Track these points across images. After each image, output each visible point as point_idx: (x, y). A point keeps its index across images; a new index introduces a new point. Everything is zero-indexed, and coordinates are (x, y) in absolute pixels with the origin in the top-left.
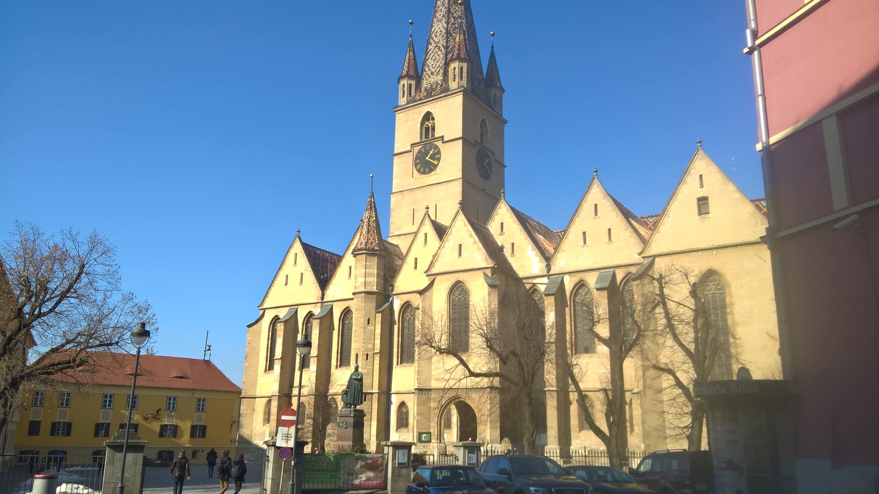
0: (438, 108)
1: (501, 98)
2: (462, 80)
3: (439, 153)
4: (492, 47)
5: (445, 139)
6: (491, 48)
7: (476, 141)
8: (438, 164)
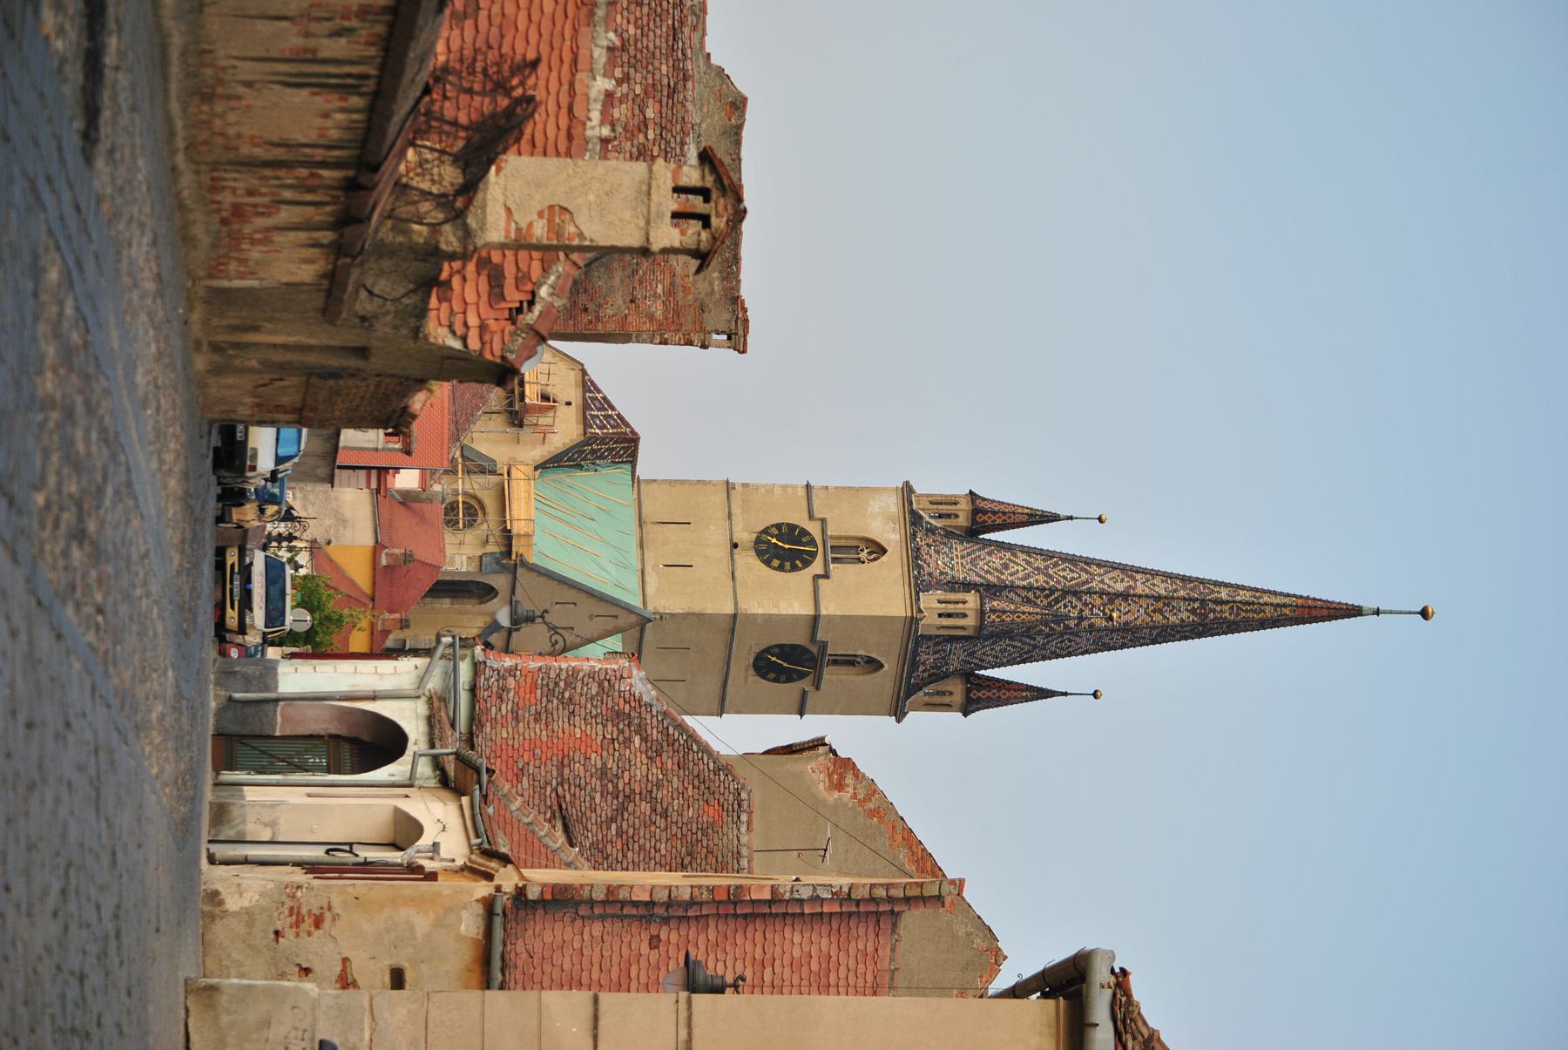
0: (892, 569)
2: (940, 615)
3: (794, 568)
4: (1066, 694)
5: (822, 582)
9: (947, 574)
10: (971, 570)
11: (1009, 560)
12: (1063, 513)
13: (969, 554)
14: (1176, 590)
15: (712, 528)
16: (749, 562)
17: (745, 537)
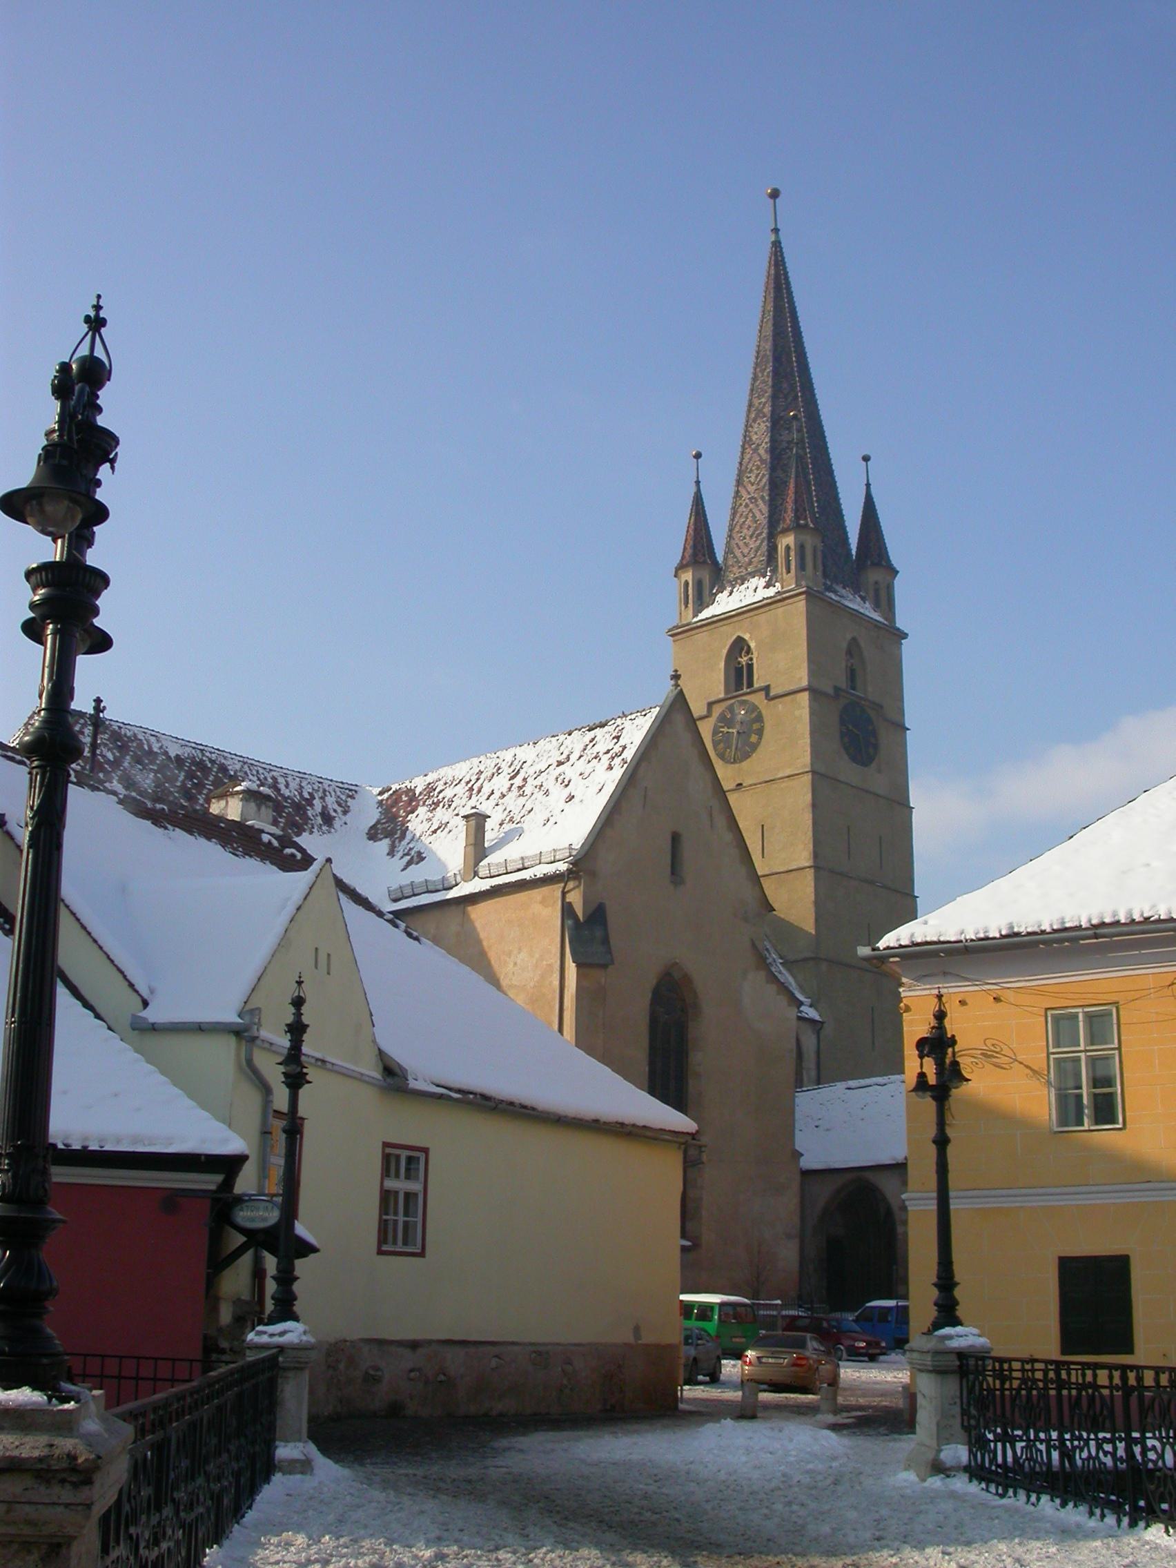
1: (890, 589)
3: (759, 719)
4: (868, 485)
5: (772, 694)
6: (865, 487)
7: (837, 689)
8: (759, 743)
12: (693, 489)
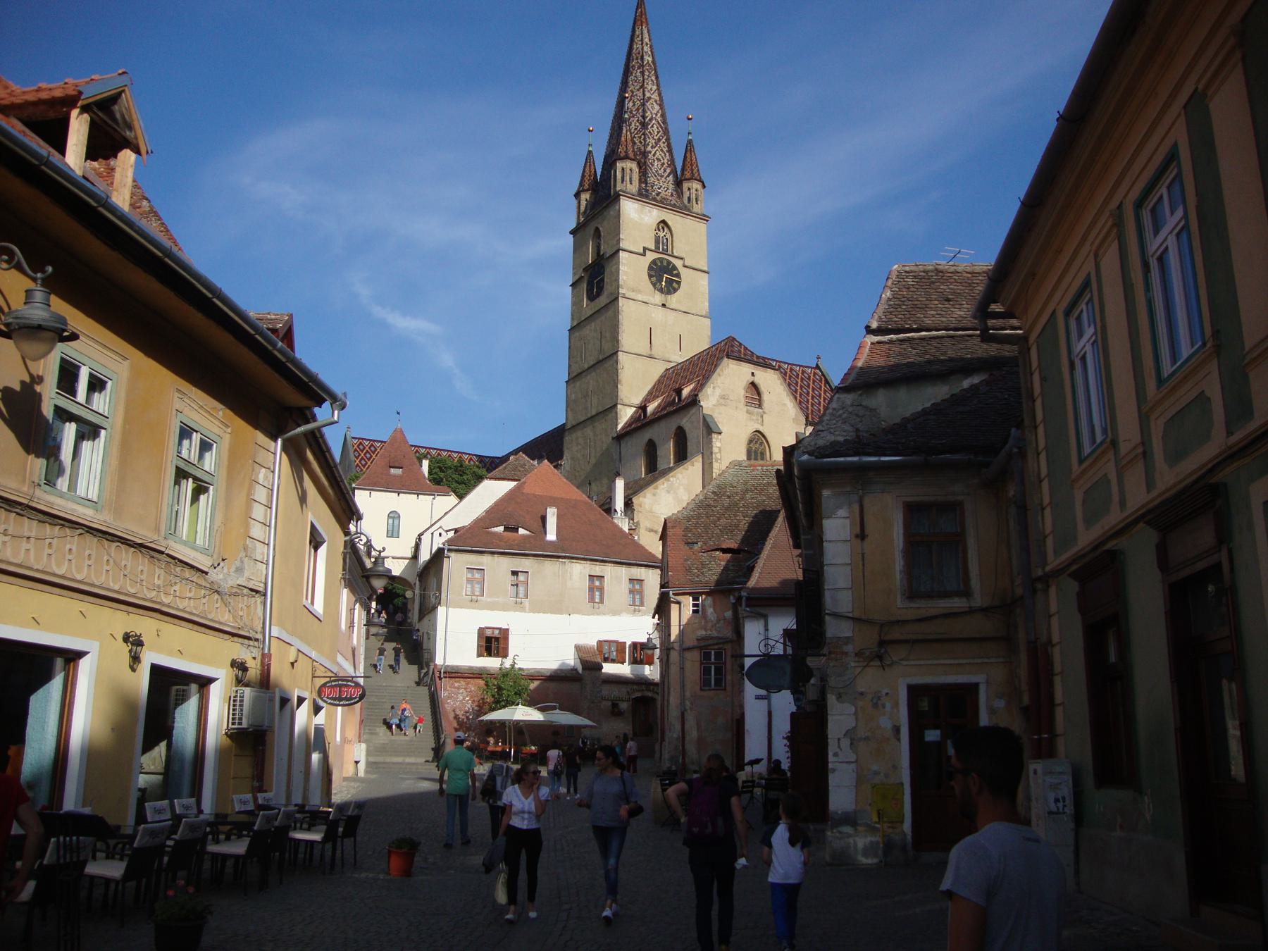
9: (672, 193)
10: (666, 178)
11: (654, 155)
13: (655, 176)
14: (652, 80)
15: (653, 315)
16: (673, 300)
17: (658, 298)
